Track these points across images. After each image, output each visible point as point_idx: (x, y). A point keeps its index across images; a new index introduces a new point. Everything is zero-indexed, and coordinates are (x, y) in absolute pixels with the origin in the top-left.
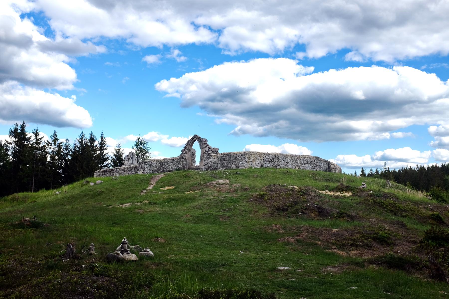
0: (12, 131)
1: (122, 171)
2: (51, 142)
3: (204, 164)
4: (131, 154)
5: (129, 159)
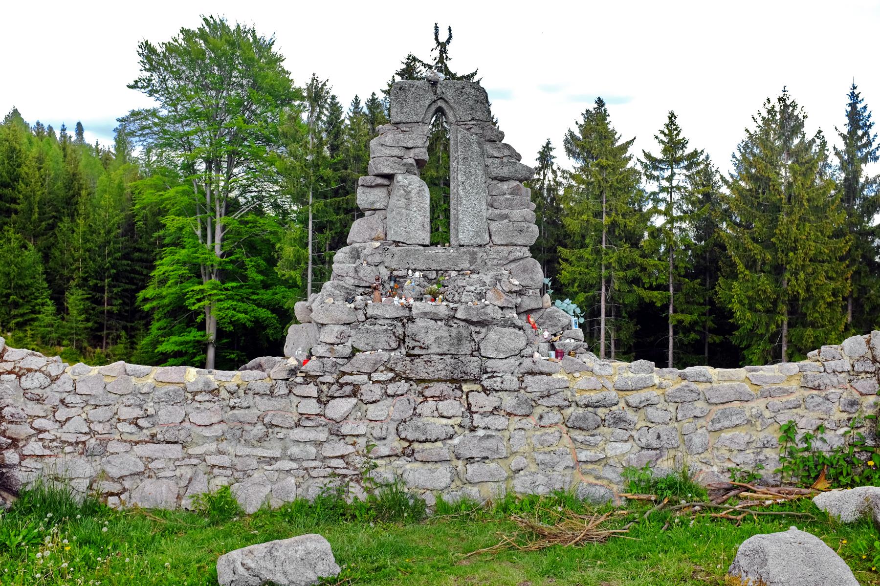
0: (572, 134)
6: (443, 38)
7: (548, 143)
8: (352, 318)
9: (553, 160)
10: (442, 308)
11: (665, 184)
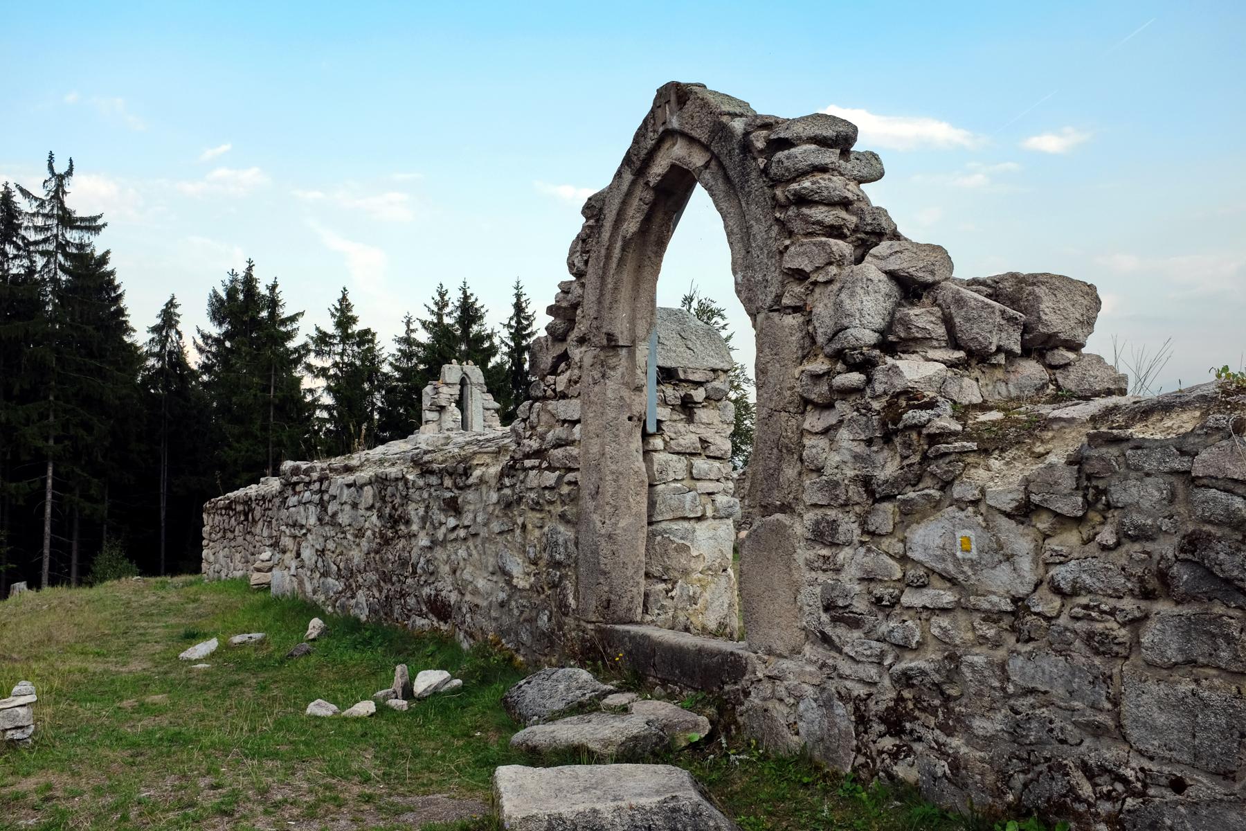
2: (330, 327)
3: (811, 597)
5: (441, 409)
6: (61, 168)
7: (173, 298)
11: (338, 358)
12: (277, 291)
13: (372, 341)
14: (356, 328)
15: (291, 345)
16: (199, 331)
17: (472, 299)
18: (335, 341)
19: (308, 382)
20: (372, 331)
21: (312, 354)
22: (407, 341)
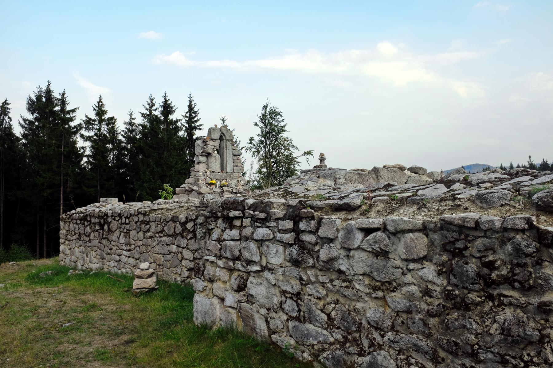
0: (30, 98)
1: (141, 234)
2: (93, 116)
4: (216, 136)
5: (208, 155)
8: (210, 192)
9: (9, 110)
10: (230, 189)
12: (65, 96)
13: (114, 123)
14: (106, 117)
15: (72, 124)
16: (21, 117)
17: (169, 102)
18: (95, 123)
19: (80, 143)
20: (115, 118)
21: (84, 129)
22: (131, 124)
